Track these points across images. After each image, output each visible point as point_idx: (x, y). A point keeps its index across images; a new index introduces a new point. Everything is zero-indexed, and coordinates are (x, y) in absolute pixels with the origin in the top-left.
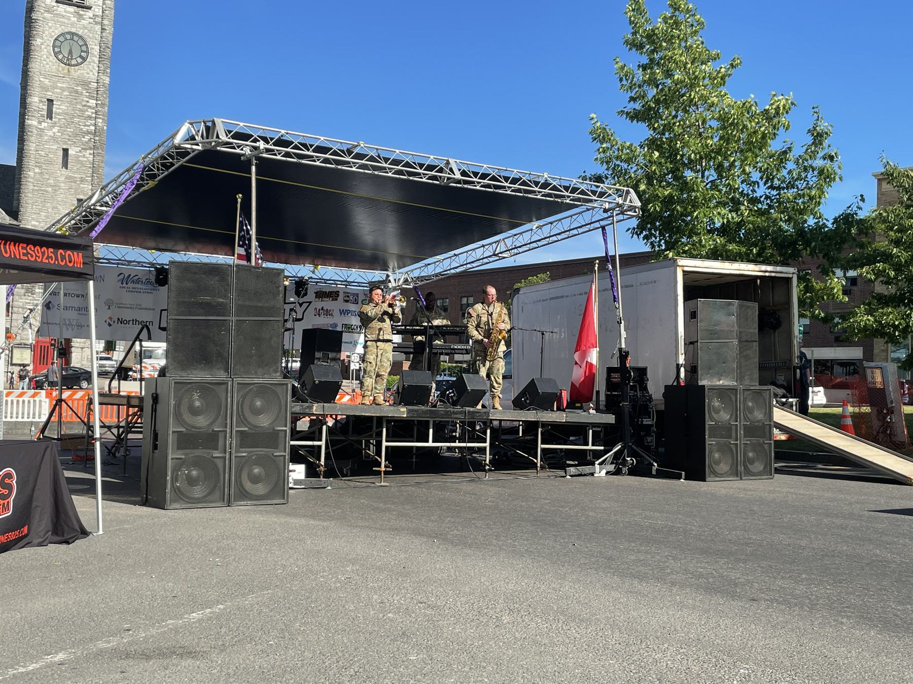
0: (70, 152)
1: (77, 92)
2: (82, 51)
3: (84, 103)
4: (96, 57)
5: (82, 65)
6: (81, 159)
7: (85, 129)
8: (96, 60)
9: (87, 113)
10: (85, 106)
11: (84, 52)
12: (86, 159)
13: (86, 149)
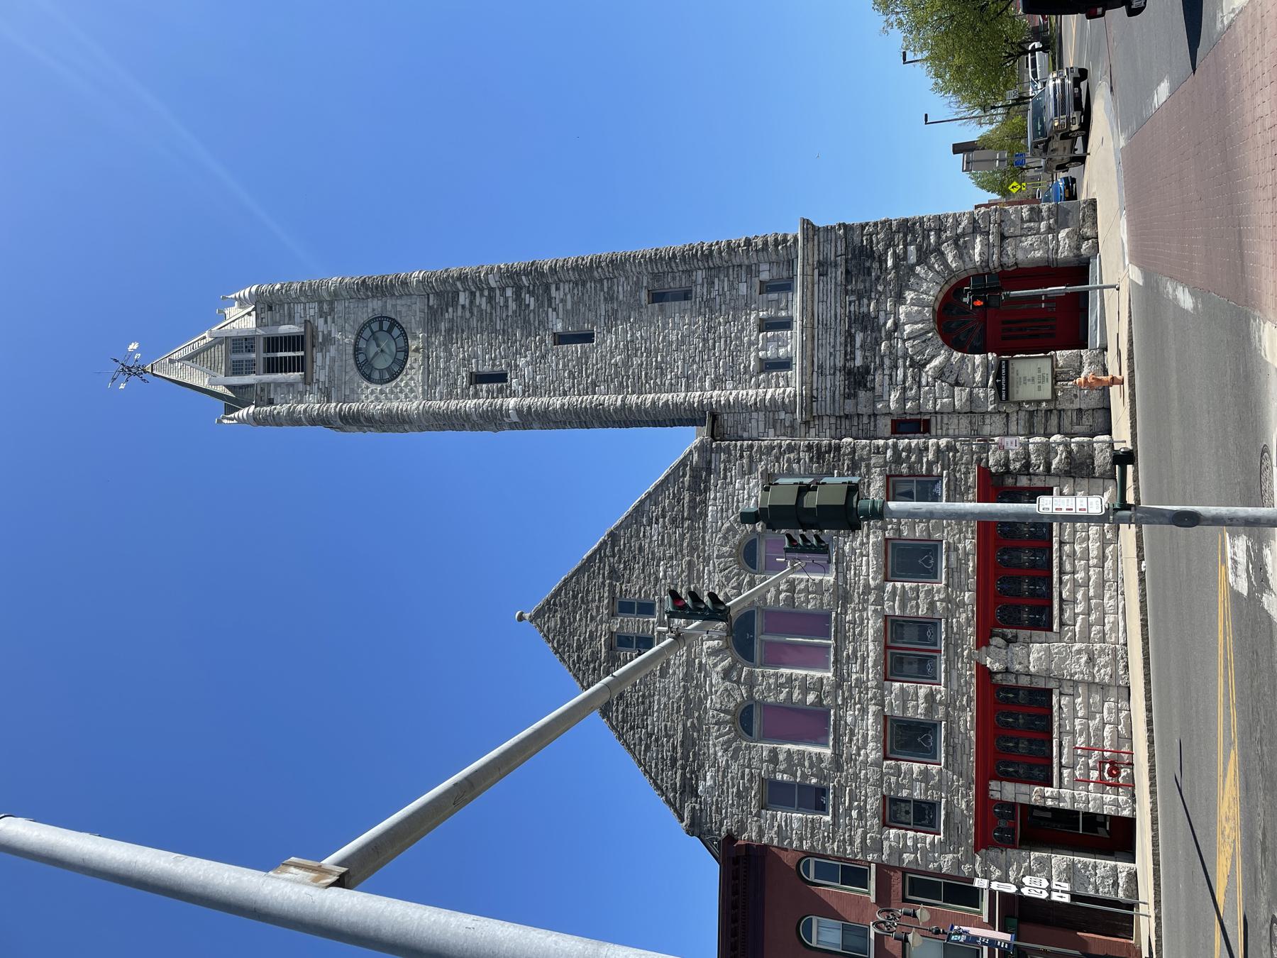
0: (559, 327)
1: (449, 331)
2: (381, 329)
3: (468, 315)
4: (386, 302)
5: (404, 326)
6: (569, 306)
7: (512, 306)
8: (390, 303)
9: (484, 306)
10: (472, 313)
11: (381, 323)
12: (569, 296)
13: (550, 299)
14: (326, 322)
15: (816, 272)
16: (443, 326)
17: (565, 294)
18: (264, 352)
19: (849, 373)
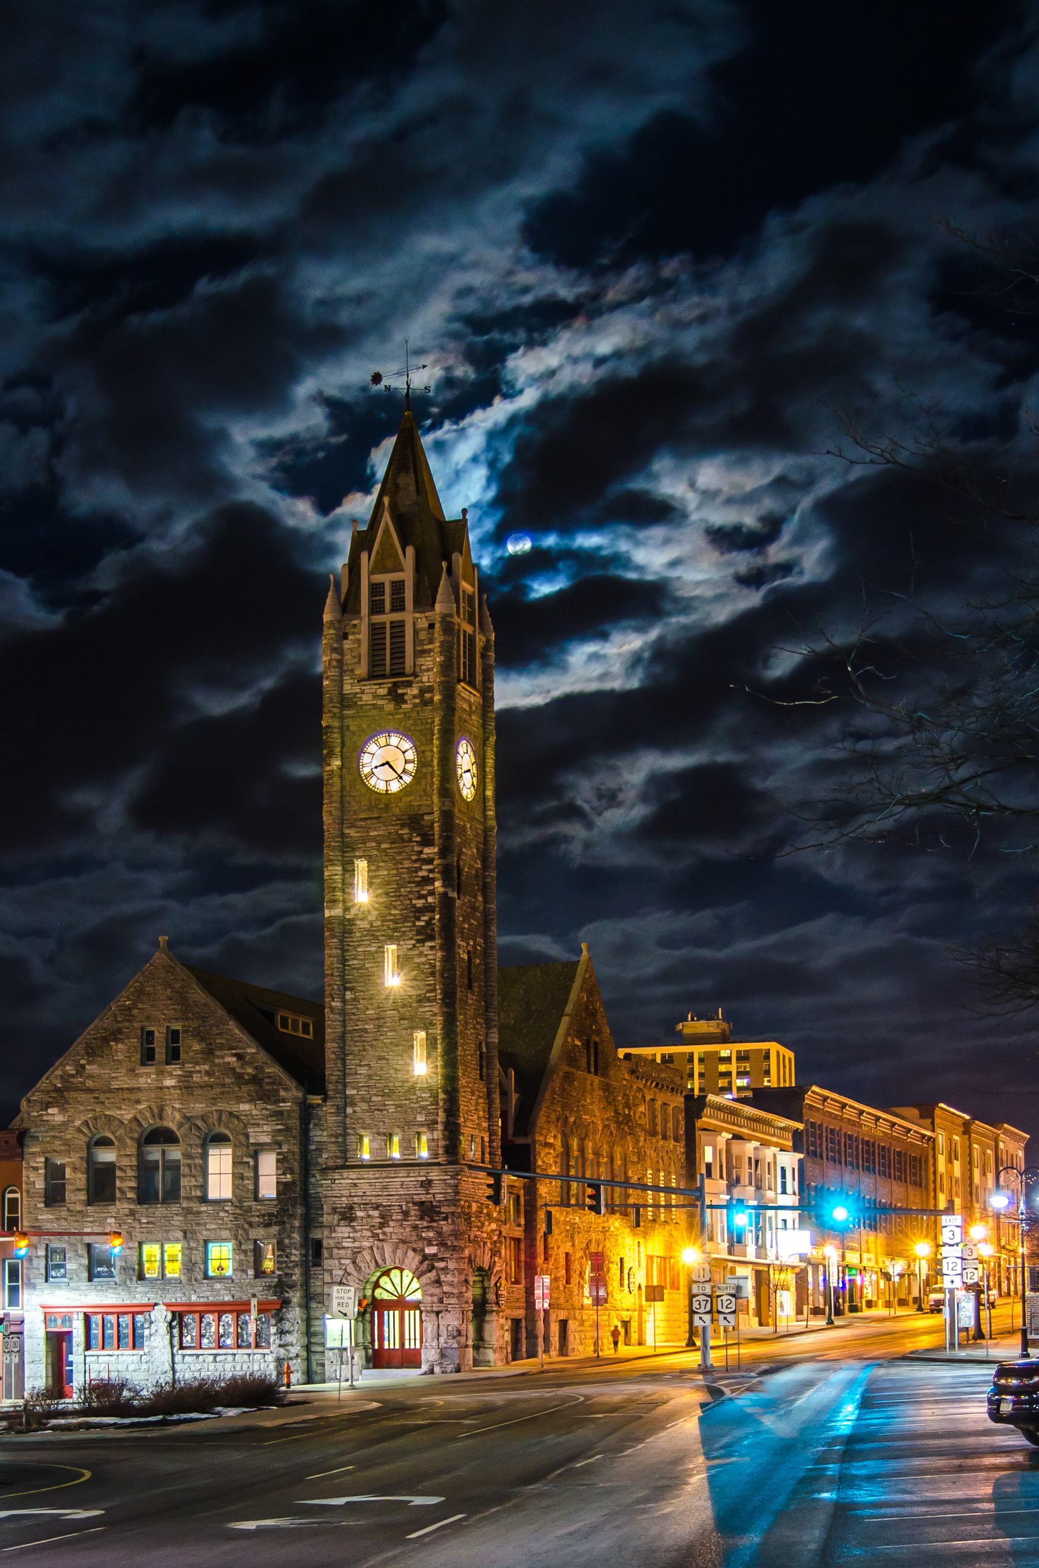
3: (414, 858)
7: (420, 903)
9: (420, 874)
14: (415, 697)
15: (425, 1179)
16: (406, 831)
17: (426, 955)
18: (391, 622)
19: (351, 1208)
